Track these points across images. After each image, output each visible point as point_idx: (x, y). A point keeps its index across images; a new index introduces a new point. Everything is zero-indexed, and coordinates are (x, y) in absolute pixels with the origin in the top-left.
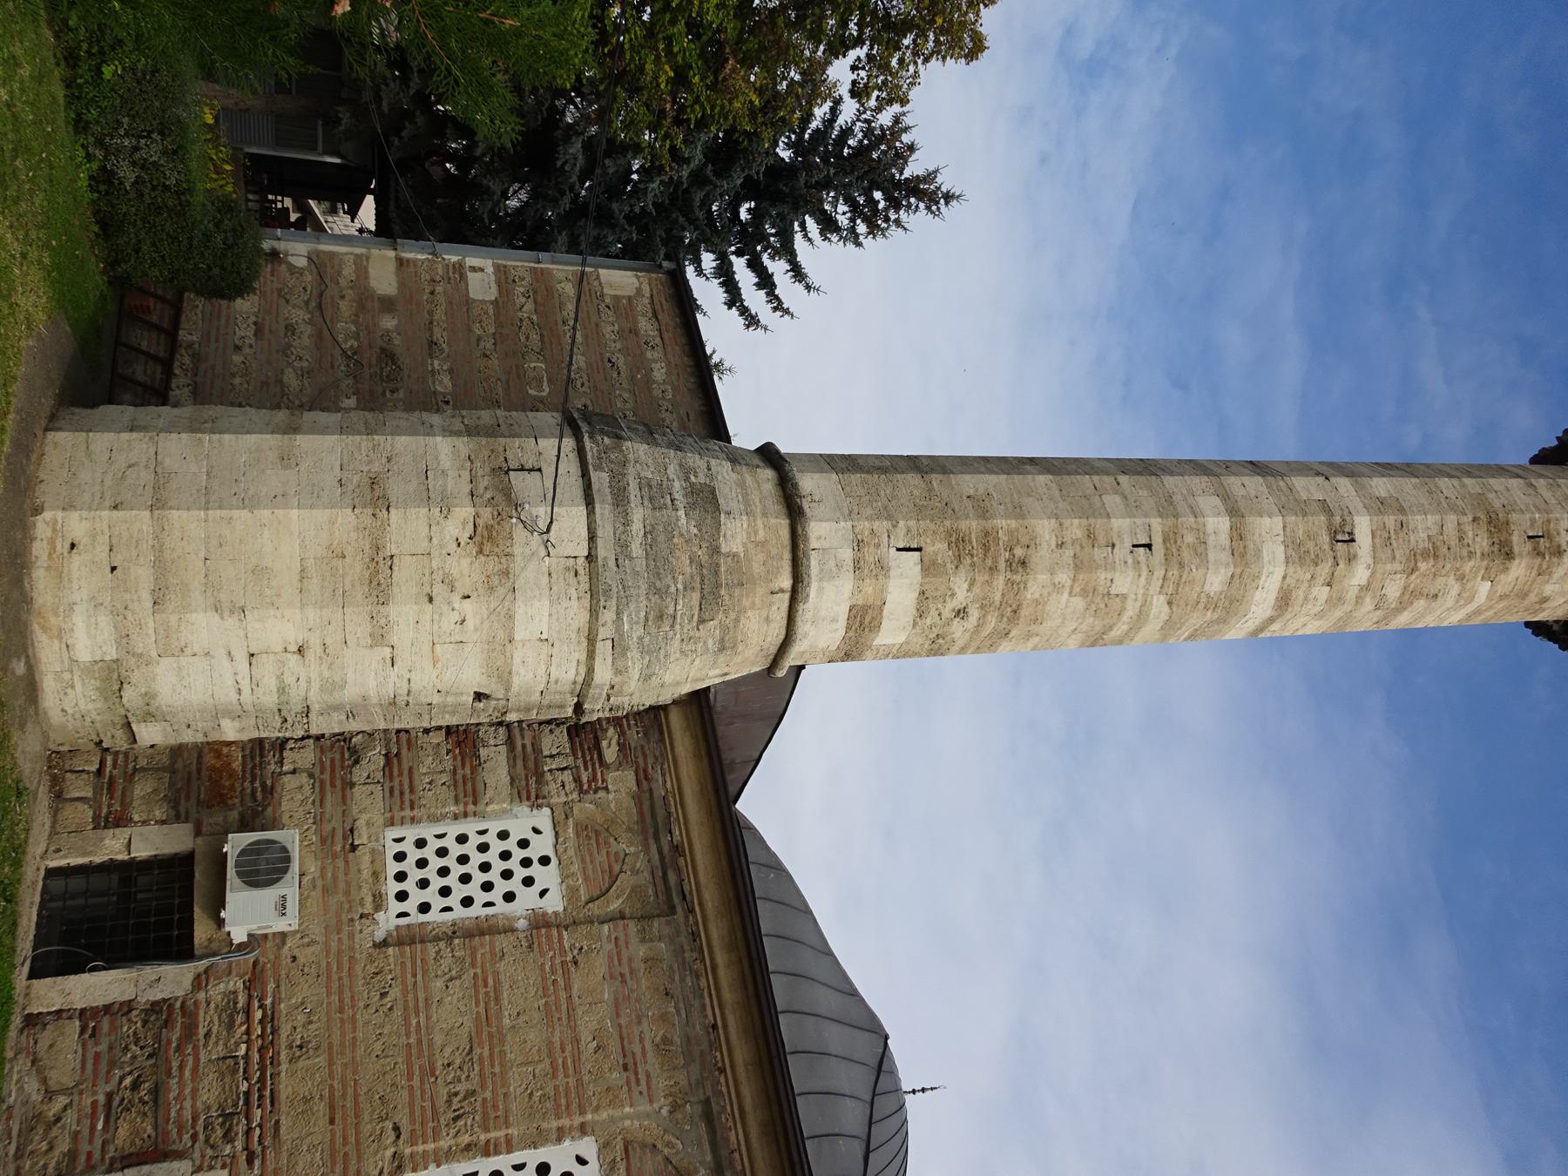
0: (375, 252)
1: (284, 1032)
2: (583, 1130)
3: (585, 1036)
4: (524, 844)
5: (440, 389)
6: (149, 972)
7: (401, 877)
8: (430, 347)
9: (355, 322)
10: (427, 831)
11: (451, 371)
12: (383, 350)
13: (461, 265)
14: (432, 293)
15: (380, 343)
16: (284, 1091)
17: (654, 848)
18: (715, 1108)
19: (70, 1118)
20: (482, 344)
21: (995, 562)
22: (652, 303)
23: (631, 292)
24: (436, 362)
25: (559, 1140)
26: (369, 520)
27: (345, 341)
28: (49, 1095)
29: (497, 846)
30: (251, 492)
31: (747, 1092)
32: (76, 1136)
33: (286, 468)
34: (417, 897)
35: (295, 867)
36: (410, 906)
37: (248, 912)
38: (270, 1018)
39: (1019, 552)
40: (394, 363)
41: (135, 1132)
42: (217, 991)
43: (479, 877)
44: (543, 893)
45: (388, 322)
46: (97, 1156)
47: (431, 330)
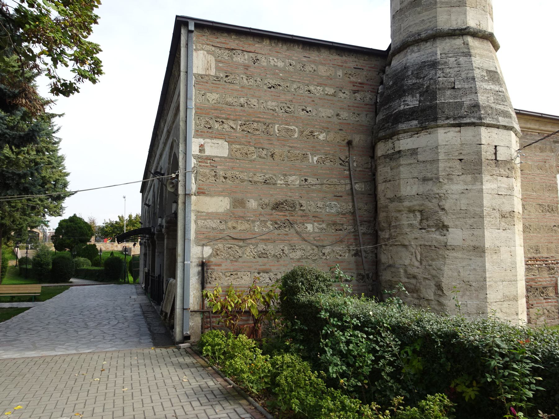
0: (193, 207)
1: (534, 255)
5: (298, 182)
8: (267, 184)
9: (253, 222)
11: (285, 175)
12: (273, 208)
13: (197, 157)
15: (268, 210)
16: (545, 255)
18: (555, 140)
19: (548, 308)
20: (263, 155)
22: (220, 48)
23: (212, 59)
24: (279, 182)
27: (268, 227)
30: (510, 265)
33: (500, 251)
40: (282, 204)
41: (552, 292)
45: (253, 204)
46: (555, 300)
47: (256, 182)
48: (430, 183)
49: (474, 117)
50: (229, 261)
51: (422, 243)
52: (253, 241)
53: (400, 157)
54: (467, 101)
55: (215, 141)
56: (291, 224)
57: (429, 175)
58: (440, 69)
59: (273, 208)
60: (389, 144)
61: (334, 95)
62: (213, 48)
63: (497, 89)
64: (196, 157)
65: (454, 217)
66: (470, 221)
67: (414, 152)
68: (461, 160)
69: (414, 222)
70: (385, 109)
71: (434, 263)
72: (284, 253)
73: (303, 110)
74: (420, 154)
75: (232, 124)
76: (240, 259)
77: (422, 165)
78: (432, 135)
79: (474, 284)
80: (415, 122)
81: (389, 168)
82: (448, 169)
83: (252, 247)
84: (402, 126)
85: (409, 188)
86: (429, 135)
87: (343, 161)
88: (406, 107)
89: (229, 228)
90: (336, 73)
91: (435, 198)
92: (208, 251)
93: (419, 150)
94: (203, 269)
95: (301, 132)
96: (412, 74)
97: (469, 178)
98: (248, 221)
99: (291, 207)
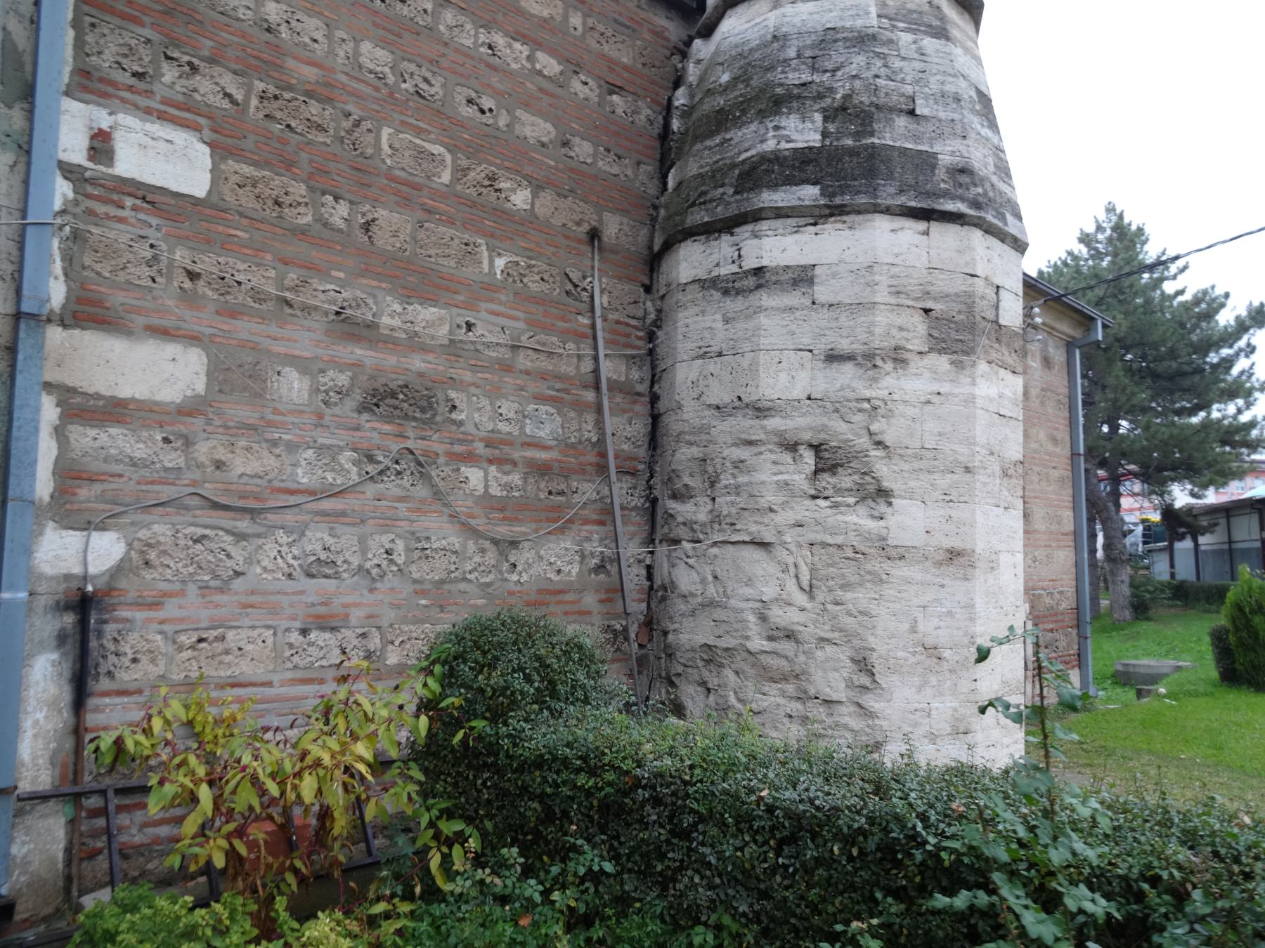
9: (292, 447)
12: (363, 408)
14: (193, 276)
27: (343, 471)
40: (393, 395)
48: (848, 367)
49: (963, 199)
50: (192, 589)
51: (818, 537)
52: (290, 517)
53: (758, 287)
54: (947, 152)
55: (157, 129)
56: (419, 464)
57: (845, 345)
58: (878, 55)
59: (363, 408)
60: (723, 247)
61: (560, 82)
64: (69, 171)
65: (906, 467)
66: (944, 481)
67: (802, 277)
68: (927, 311)
69: (796, 477)
70: (710, 148)
71: (849, 595)
72: (392, 561)
73: (470, 101)
74: (822, 284)
75: (229, 82)
76: (238, 583)
77: (825, 313)
78: (857, 233)
79: (947, 654)
81: (718, 317)
82: (895, 332)
83: (284, 539)
85: (783, 377)
86: (847, 232)
87: (576, 286)
88: (784, 145)
89: (200, 466)
91: (860, 410)
92: (106, 550)
93: (818, 271)
94: (83, 624)
95: (460, 172)
96: (799, 56)
97: (942, 362)
98: (274, 443)
99: (423, 410)
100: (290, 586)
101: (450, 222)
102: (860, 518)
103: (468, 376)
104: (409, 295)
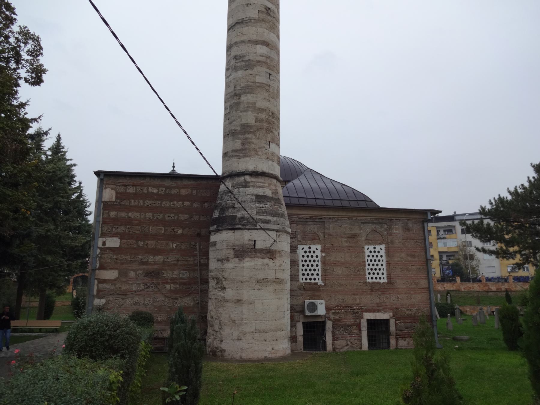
2: (363, 248)
3: (347, 245)
4: (305, 252)
6: (327, 329)
7: (310, 279)
9: (132, 284)
10: (301, 273)
12: (144, 276)
14: (117, 259)
17: (309, 223)
19: (352, 341)
21: (272, 121)
22: (119, 186)
23: (114, 192)
25: (365, 253)
26: (269, 283)
28: (347, 345)
29: (306, 258)
31: (362, 215)
32: (355, 339)
34: (315, 276)
35: (313, 301)
36: (317, 277)
37: (321, 310)
38: (338, 306)
39: (270, 114)
41: (355, 329)
42: (332, 316)
43: (312, 263)
44: (317, 249)
55: (112, 238)
62: (115, 186)
63: (261, 206)
64: (100, 248)
66: (236, 285)
73: (169, 216)
79: (237, 322)
80: (215, 226)
83: (130, 299)
84: (212, 228)
90: (192, 192)
95: (165, 230)
100: (131, 307)
101: (164, 240)
102: (221, 294)
103: (167, 268)
104: (154, 255)
